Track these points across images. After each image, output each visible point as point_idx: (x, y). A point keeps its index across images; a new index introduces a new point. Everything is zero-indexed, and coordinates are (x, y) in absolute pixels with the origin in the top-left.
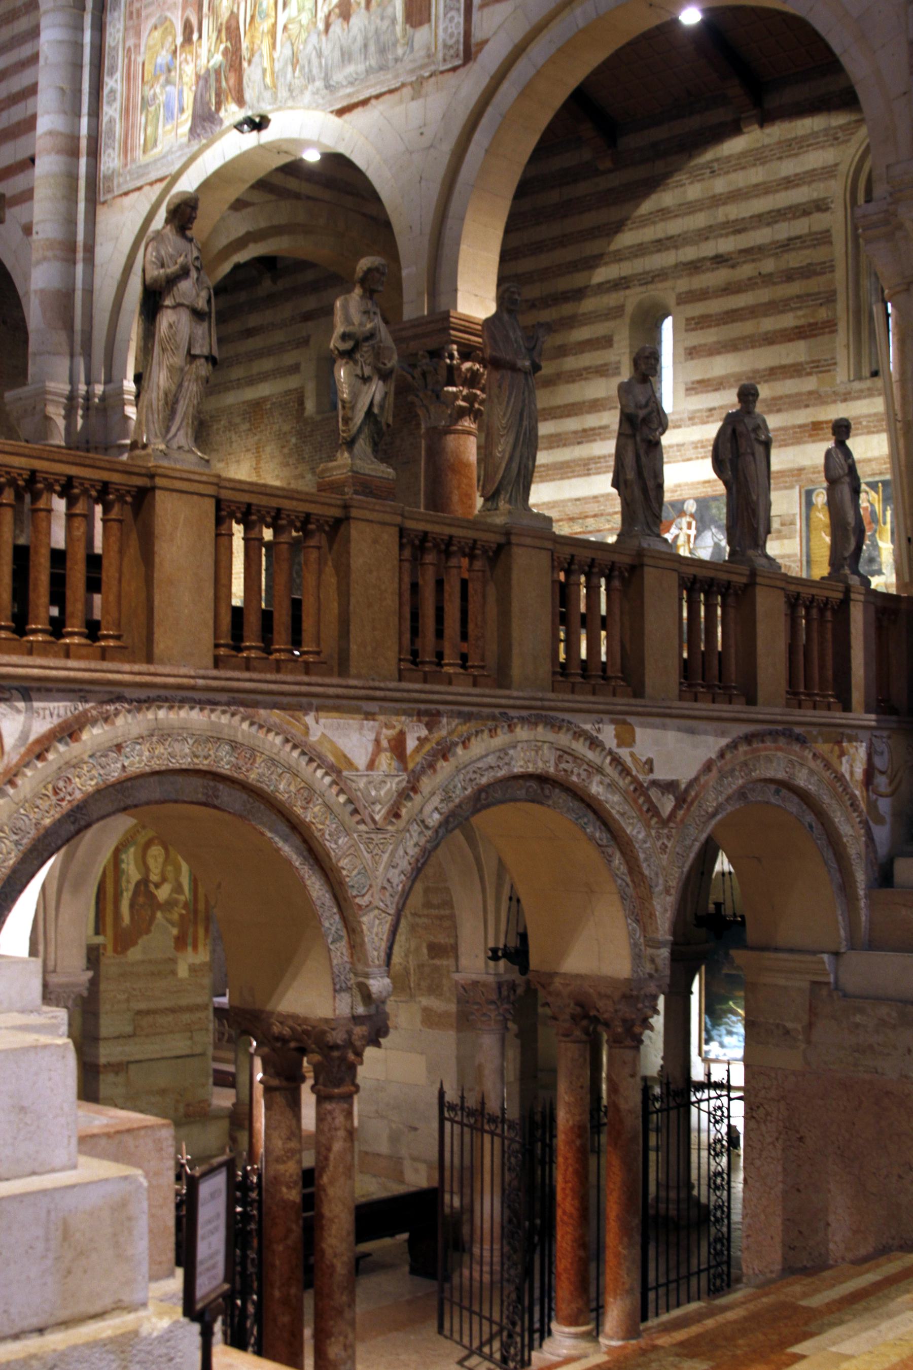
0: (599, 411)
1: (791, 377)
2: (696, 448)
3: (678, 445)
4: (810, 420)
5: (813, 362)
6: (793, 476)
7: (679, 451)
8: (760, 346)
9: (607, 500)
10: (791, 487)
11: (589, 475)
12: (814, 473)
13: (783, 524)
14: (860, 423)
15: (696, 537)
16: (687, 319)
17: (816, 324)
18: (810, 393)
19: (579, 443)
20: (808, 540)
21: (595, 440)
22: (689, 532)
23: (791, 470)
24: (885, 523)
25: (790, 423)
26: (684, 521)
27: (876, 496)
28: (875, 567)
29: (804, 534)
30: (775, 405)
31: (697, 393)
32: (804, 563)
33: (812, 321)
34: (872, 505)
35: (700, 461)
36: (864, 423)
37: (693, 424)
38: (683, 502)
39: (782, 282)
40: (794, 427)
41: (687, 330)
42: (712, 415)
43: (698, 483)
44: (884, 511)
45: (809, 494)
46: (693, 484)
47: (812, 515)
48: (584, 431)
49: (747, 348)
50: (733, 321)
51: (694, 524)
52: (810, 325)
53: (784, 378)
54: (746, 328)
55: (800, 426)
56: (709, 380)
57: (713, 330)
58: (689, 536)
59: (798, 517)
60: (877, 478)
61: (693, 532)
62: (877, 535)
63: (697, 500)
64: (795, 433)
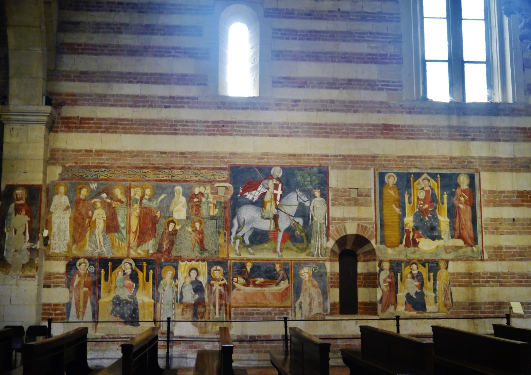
0: (188, 84)
1: (366, 89)
2: (282, 127)
3: (265, 123)
4: (382, 122)
5: (383, 81)
6: (368, 160)
7: (266, 128)
8: (339, 62)
9: (195, 157)
10: (367, 168)
11: (176, 134)
12: (385, 160)
13: (359, 195)
14: (422, 131)
15: (282, 197)
16: (274, 29)
17: (387, 55)
18: (381, 103)
19: (166, 107)
20: (381, 210)
21: (183, 107)
22: (275, 192)
23: (366, 156)
24: (443, 203)
25: (365, 122)
26: (271, 183)
27: (436, 184)
28: (436, 234)
29: (378, 204)
30: (353, 107)
31: (283, 86)
32: (378, 226)
33: (382, 52)
34: (432, 189)
35: (286, 138)
36: (425, 131)
37: (280, 109)
38: (270, 168)
39: (357, 20)
40: (368, 125)
41: (273, 37)
42: (297, 105)
43: (284, 155)
44: (442, 195)
45: (382, 175)
46: (278, 155)
47: (385, 191)
48: (172, 97)
49: (328, 61)
50: (315, 39)
51: (280, 186)
52: (381, 55)
53: (360, 89)
54: (328, 46)
55: (373, 125)
56: (294, 78)
57: (298, 42)
58: (276, 195)
59: (373, 191)
60: (436, 171)
61: (279, 192)
62: (437, 211)
63: (283, 168)
64: (370, 129)
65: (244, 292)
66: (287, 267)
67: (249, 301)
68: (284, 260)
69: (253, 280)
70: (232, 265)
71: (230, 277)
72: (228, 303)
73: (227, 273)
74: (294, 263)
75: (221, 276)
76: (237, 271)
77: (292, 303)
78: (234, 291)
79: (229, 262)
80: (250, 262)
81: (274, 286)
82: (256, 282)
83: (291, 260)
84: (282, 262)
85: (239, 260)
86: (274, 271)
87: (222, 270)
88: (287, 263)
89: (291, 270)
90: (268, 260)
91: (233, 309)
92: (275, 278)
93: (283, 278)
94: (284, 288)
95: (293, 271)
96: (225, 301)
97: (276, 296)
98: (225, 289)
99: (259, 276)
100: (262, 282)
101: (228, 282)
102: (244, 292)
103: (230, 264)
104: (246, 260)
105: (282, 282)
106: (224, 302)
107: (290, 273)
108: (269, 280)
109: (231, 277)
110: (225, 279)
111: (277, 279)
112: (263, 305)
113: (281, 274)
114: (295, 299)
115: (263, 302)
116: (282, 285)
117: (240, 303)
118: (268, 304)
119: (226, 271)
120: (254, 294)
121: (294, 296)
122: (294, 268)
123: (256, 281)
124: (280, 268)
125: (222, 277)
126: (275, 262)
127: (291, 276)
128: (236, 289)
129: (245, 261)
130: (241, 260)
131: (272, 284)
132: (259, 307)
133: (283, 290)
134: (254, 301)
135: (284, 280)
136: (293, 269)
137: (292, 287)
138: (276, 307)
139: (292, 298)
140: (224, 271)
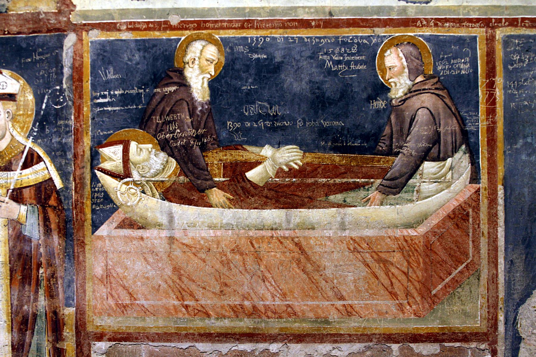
65: (171, 240)
66: (464, 68)
67: (207, 301)
68: (439, 22)
69: (230, 156)
70: (87, 60)
71: (77, 141)
72: (69, 312)
73: (58, 115)
74: (507, 41)
75: (21, 139)
76: (125, 99)
77: (493, 307)
78: (103, 230)
79: (70, 40)
80: (211, 40)
81: (374, 194)
82: (251, 175)
83: (486, 23)
84: (428, 32)
85: (133, 27)
86: (371, 98)
87: (30, 97)
88: (460, 41)
89: (491, 85)
90: (328, 24)
91: (102, 346)
92: (382, 146)
93: (436, 139)
94: (443, 214)
95: (499, 94)
96: (51, 295)
97: (384, 262)
98: (46, 220)
99: (273, 129)
100: (292, 172)
101: (64, 176)
102: (171, 240)
103: (78, 55)
104: (183, 26)
105: (428, 167)
106: (42, 302)
107: (482, 107)
108: (336, 158)
109: (87, 142)
110: (48, 153)
111: (391, 152)
112: (297, 326)
113: (422, 116)
114: (519, 287)
115: (298, 305)
116: (427, 187)
117: (145, 311)
118: (334, 316)
119: (55, 98)
120: (236, 250)
121: (510, 264)
122: (509, 75)
123: (252, 165)
124: (414, 72)
125: (29, 144)
126: (381, 31)
127: (491, 130)
128: (117, 217)
129: (173, 35)
130: (149, 27)
131: (357, 187)
132: (272, 338)
133: (434, 221)
134: (236, 301)
135: (437, 159)
136: (499, 80)
137: (493, 201)
138: (390, 338)
139: (493, 279)
140: (39, 100)
